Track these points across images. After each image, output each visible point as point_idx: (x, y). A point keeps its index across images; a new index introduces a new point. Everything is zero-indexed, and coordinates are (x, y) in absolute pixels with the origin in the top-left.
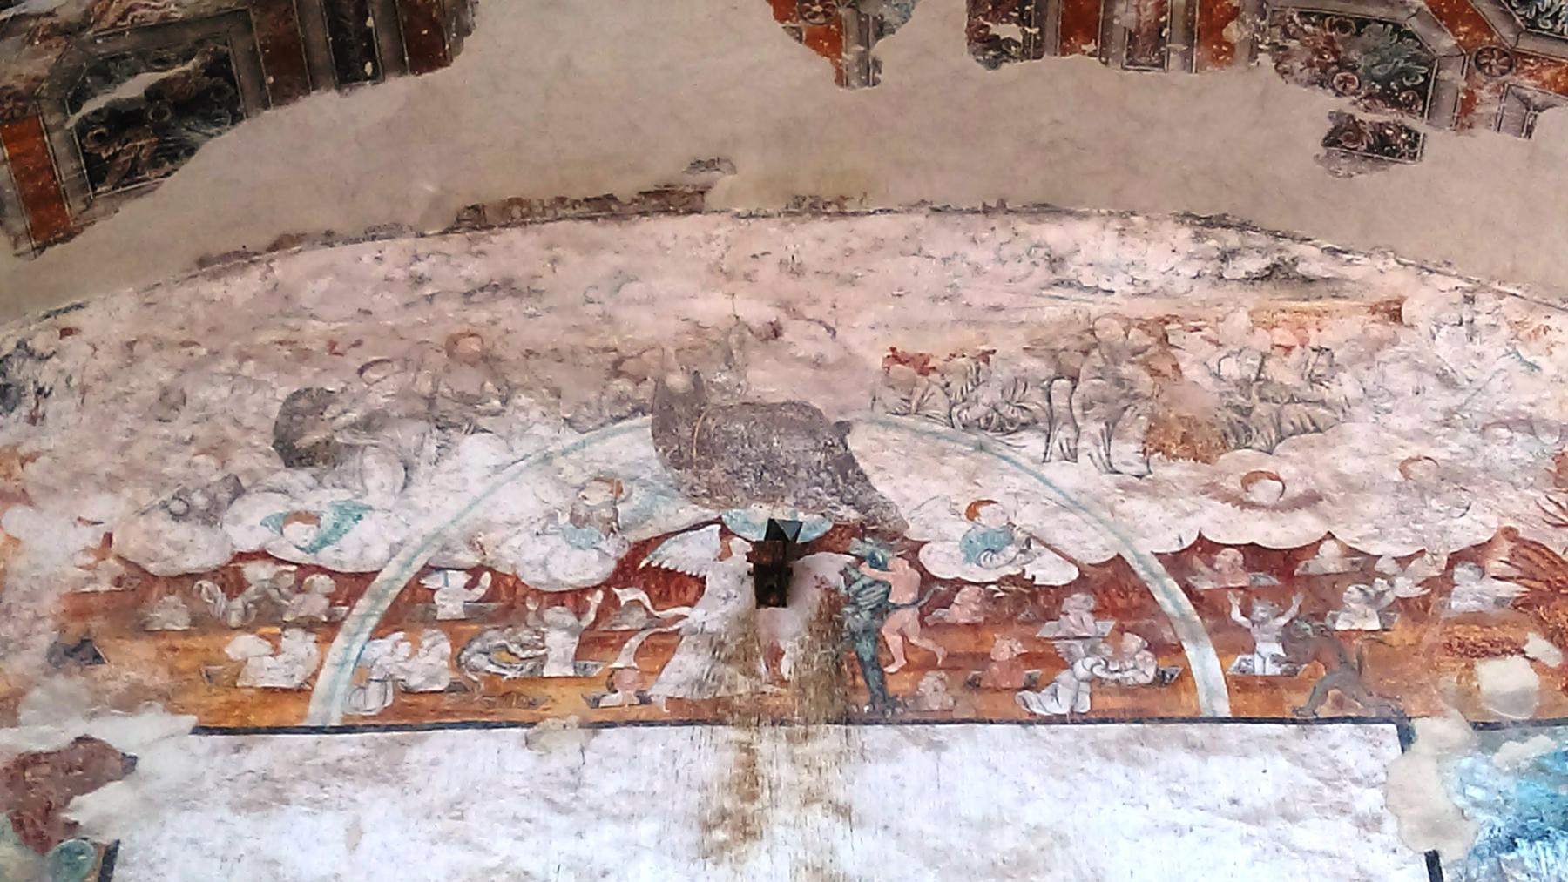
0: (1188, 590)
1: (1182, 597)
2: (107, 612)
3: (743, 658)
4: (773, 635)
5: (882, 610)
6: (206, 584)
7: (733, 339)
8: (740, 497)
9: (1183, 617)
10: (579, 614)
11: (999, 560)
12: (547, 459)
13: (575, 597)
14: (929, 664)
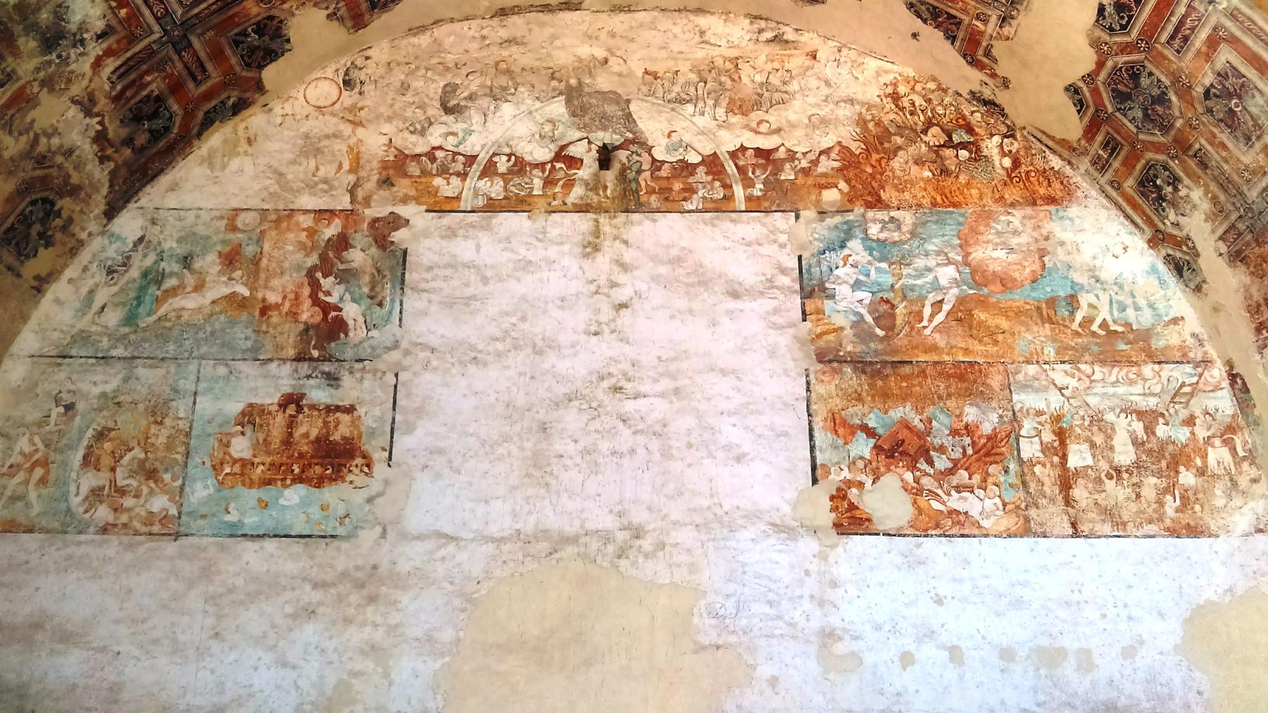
0: (736, 165)
1: (734, 167)
2: (394, 168)
3: (595, 189)
4: (605, 181)
5: (639, 172)
6: (424, 158)
7: (591, 65)
9: (734, 175)
10: (543, 171)
11: (677, 153)
12: (530, 113)
13: (541, 166)
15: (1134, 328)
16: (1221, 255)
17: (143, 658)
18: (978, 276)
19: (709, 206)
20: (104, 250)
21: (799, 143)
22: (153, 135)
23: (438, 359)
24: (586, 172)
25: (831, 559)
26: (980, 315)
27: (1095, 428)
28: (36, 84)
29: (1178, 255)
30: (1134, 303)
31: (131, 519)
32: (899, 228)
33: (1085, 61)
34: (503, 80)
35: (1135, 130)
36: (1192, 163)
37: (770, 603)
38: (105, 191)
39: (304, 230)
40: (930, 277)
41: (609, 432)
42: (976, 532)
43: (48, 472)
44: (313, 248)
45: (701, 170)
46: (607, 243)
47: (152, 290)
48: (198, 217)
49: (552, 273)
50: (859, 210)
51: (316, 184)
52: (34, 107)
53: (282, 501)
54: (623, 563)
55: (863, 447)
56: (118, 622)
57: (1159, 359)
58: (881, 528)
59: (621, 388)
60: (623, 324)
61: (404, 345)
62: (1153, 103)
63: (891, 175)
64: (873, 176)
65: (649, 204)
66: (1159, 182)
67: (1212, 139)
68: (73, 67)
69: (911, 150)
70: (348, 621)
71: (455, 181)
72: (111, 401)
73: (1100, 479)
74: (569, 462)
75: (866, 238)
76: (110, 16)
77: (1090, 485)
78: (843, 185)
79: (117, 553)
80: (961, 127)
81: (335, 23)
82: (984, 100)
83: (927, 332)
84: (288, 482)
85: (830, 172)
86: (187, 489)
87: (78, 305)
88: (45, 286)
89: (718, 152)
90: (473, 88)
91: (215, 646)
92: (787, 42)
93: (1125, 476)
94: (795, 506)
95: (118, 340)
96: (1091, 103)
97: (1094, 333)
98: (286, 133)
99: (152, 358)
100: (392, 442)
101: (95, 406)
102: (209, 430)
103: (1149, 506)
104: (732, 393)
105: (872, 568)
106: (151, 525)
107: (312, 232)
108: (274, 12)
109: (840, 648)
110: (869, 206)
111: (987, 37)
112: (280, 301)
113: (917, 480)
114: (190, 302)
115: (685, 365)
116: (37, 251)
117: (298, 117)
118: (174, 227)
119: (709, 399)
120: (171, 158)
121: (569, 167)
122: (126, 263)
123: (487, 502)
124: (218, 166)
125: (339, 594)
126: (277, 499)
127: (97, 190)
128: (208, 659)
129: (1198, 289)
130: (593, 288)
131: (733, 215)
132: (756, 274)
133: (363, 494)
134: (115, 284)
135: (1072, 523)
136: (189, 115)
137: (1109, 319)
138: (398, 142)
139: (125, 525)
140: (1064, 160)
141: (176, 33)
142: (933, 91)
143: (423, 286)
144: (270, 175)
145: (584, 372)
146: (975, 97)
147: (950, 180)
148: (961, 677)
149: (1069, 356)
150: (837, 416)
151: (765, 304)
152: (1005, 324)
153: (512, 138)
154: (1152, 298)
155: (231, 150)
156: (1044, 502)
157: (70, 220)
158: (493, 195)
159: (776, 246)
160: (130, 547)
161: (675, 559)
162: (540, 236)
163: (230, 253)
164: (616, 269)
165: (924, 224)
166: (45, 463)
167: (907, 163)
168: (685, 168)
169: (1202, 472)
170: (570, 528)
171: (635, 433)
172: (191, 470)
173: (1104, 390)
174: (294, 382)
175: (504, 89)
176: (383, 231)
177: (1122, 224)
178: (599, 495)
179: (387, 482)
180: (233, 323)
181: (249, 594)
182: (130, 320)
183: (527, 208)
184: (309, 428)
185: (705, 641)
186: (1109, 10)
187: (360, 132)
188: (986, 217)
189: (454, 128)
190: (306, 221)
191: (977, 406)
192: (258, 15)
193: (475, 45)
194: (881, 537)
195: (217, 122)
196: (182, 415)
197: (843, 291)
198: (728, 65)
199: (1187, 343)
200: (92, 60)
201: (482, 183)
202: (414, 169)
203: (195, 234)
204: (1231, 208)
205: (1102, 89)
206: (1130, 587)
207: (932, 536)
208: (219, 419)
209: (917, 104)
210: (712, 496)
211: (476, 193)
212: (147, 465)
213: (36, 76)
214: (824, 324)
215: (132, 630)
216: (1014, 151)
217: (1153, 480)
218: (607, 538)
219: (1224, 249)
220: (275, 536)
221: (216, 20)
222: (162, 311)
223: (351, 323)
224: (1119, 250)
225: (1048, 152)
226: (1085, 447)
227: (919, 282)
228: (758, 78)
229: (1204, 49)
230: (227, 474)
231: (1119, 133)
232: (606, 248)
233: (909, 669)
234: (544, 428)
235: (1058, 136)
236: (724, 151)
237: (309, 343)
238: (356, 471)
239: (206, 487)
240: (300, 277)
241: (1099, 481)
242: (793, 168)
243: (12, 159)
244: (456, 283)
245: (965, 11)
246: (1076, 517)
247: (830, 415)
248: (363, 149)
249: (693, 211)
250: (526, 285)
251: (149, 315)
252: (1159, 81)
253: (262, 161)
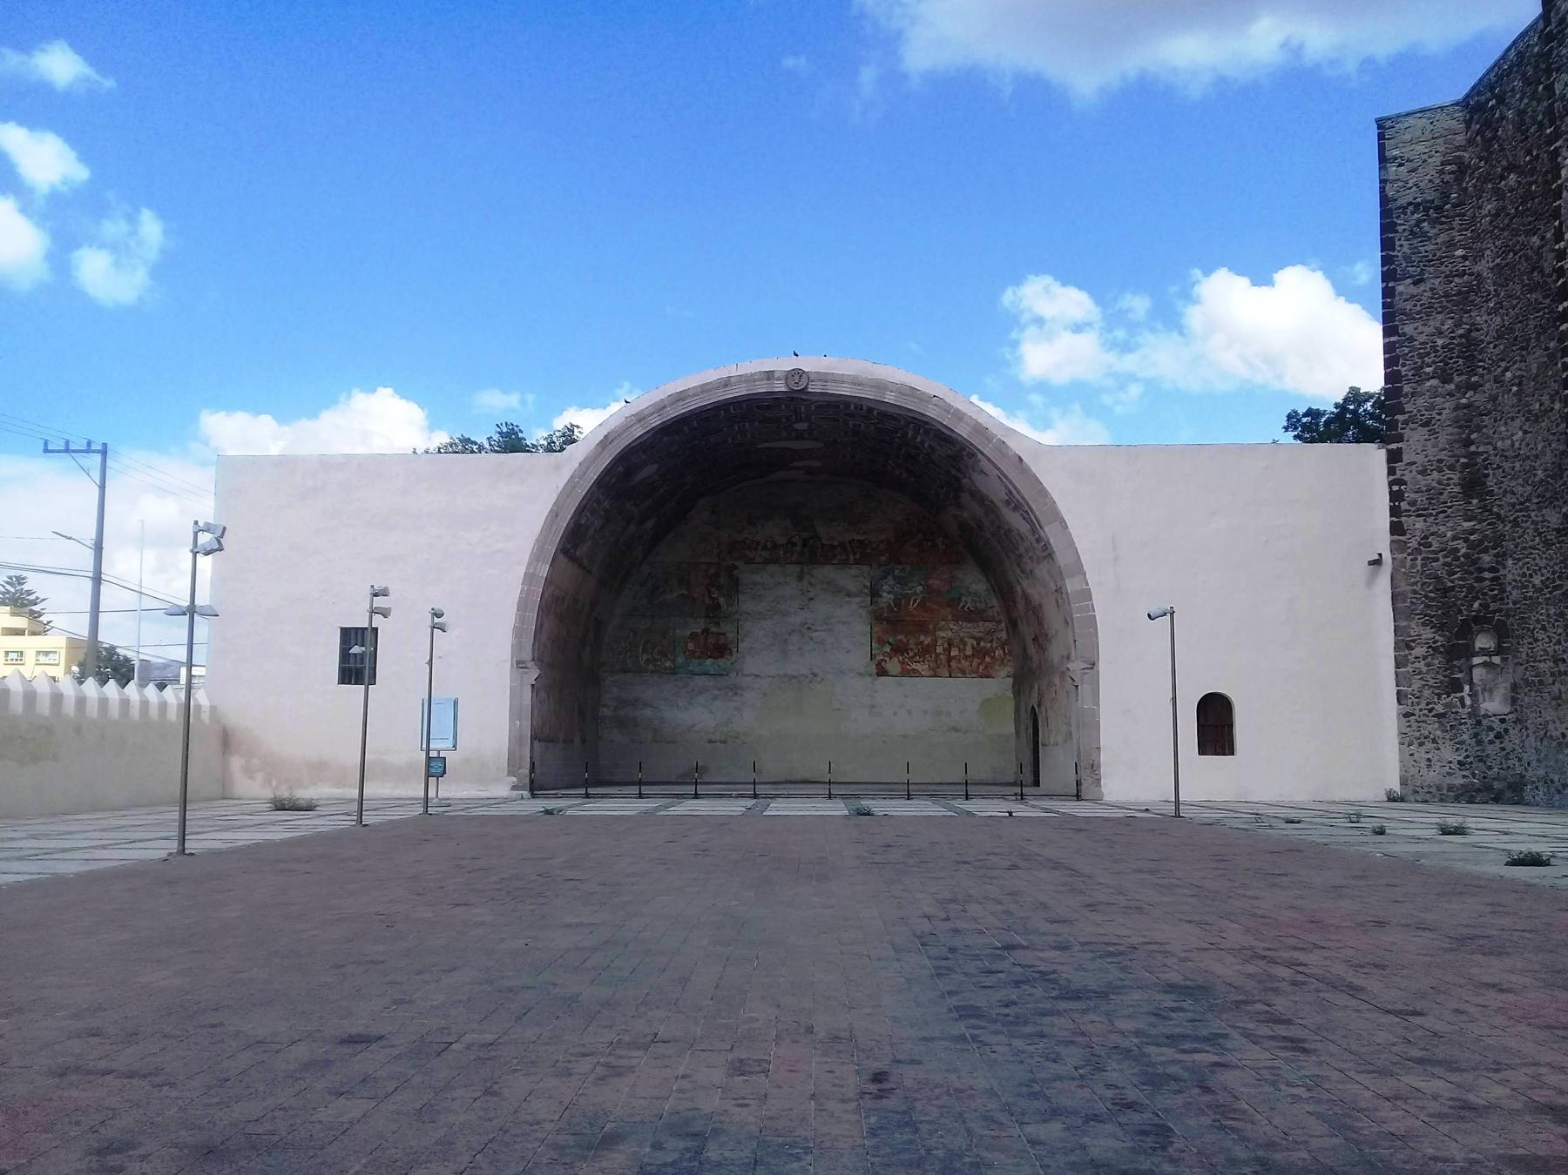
24: (798, 549)
26: (928, 604)
40: (913, 590)
46: (806, 577)
54: (811, 685)
55: (888, 649)
71: (754, 553)
75: (895, 578)
78: (887, 555)
149: (956, 620)
151: (858, 599)
152: (935, 607)
168: (833, 547)
169: (992, 658)
184: (711, 640)
197: (885, 594)
218: (806, 676)
234: (785, 641)
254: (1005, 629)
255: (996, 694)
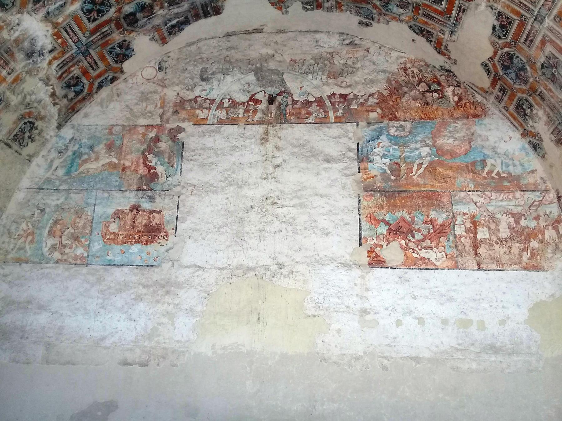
0: (330, 102)
4: (271, 110)
5: (287, 106)
6: (192, 101)
8: (267, 86)
9: (329, 106)
10: (244, 106)
11: (304, 97)
12: (239, 80)
13: (243, 104)
14: (293, 114)
15: (513, 175)
16: (552, 141)
17: (72, 316)
18: (440, 151)
19: (318, 121)
20: (57, 143)
21: (359, 92)
22: (76, 93)
23: (196, 190)
24: (263, 105)
25: (367, 279)
27: (491, 221)
28: (24, 73)
29: (534, 141)
30: (513, 163)
31: (68, 257)
32: (404, 130)
33: (489, 52)
34: (227, 66)
35: (512, 83)
36: (538, 98)
37: (339, 298)
38: (56, 117)
39: (141, 134)
40: (417, 152)
41: (270, 222)
42: (433, 267)
43: (34, 238)
44: (144, 142)
45: (315, 104)
46: (271, 138)
47: (78, 161)
48: (96, 128)
49: (246, 152)
50: (386, 122)
51: (146, 114)
52: (24, 83)
53: (130, 251)
55: (383, 229)
56: (62, 300)
57: (523, 190)
58: (389, 265)
59: (276, 203)
60: (277, 175)
61: (182, 184)
62: (519, 71)
63: (401, 106)
64: (393, 106)
65: (291, 120)
66: (524, 107)
67: (546, 87)
68: (39, 65)
69: (412, 94)
70: (158, 302)
71: (206, 111)
72: (60, 208)
73: (492, 244)
74: (252, 236)
75: (389, 134)
76: (53, 41)
77: (487, 247)
78: (379, 110)
79: (63, 272)
80: (435, 82)
81: (154, 42)
82: (446, 70)
83: (415, 177)
84: (133, 243)
85: (374, 105)
86: (91, 245)
87: (46, 167)
88: (33, 159)
89: (322, 96)
90: (214, 69)
91: (102, 311)
92: (356, 44)
93: (504, 243)
94: (351, 255)
95: (63, 182)
96: (493, 71)
97: (493, 177)
98: (134, 91)
99: (77, 190)
100: (176, 226)
101: (53, 210)
102: (100, 220)
103: (515, 256)
104: (325, 205)
105: (385, 283)
106: (76, 260)
107: (144, 135)
108: (126, 38)
109: (369, 317)
110: (391, 120)
111: (445, 40)
112: (130, 164)
113: (407, 244)
114: (93, 166)
115: (304, 193)
116: (28, 144)
117: (139, 84)
118: (86, 133)
119: (315, 208)
120: (85, 103)
121: (255, 104)
122: (66, 149)
123: (216, 252)
124: (105, 106)
125: (154, 290)
126: (128, 250)
127: (53, 117)
128: (99, 317)
129: (543, 157)
130: (264, 158)
131: (328, 125)
132: (338, 152)
133: (163, 249)
134: (62, 158)
135: (478, 264)
136: (91, 85)
137: (500, 171)
138: (181, 94)
139: (65, 260)
140: (483, 97)
141: (83, 49)
142: (423, 66)
143: (191, 158)
144: (127, 110)
145: (260, 196)
146: (442, 68)
147: (429, 108)
148: (423, 331)
149: (481, 188)
150: (372, 215)
151: (341, 165)
153: (231, 92)
154: (522, 161)
155: (110, 99)
156: (464, 254)
157: (42, 130)
158: (221, 117)
159: (347, 139)
160: (67, 269)
161: (297, 278)
162: (242, 135)
163: (109, 144)
164: (275, 149)
165: (416, 128)
166: (33, 234)
167: (409, 100)
168: (308, 104)
169: (541, 241)
170: (252, 264)
171: (281, 223)
172: (93, 238)
173: (497, 204)
174: (135, 200)
175: (228, 69)
176: (174, 134)
177: (509, 126)
178: (265, 250)
179: (175, 244)
180: (111, 174)
181: (116, 290)
182: (68, 173)
183: (236, 123)
184: (142, 220)
185: (310, 313)
186: (498, 28)
187: (165, 90)
188: (445, 124)
189: (205, 88)
190: (141, 130)
191: (436, 211)
192: (119, 40)
193: (216, 50)
194: (389, 269)
195: (104, 87)
196: (89, 214)
197: (377, 158)
198: (329, 56)
199: (538, 182)
200: (47, 61)
201: (217, 111)
202: (188, 106)
203: (95, 136)
204: (556, 119)
205: (497, 64)
206: (504, 293)
207: (412, 269)
208: (105, 216)
209: (415, 72)
210: (314, 251)
211: (214, 117)
212: (75, 235)
213: (23, 69)
214: (369, 174)
215: (68, 304)
216: (459, 93)
217: (518, 245)
219: (553, 138)
220: (128, 265)
221: (100, 42)
222: (81, 169)
223: (160, 174)
224: (507, 139)
225: (475, 93)
226: (486, 229)
227: (412, 155)
228: (342, 62)
229: (540, 45)
230: (107, 239)
231: (505, 84)
232: (271, 140)
233: (400, 327)
234: (241, 220)
235: (480, 86)
236: (325, 95)
237: (142, 183)
238: (161, 238)
239: (99, 244)
240: (139, 154)
241: (491, 245)
242: (356, 103)
243: (15, 105)
244: (205, 157)
245: (434, 29)
246: (479, 261)
247: (369, 215)
248: (166, 98)
249: (310, 123)
250: (235, 158)
251: (76, 171)
252: (521, 60)
253: (123, 103)
254: (556, 200)
255: (553, 296)
